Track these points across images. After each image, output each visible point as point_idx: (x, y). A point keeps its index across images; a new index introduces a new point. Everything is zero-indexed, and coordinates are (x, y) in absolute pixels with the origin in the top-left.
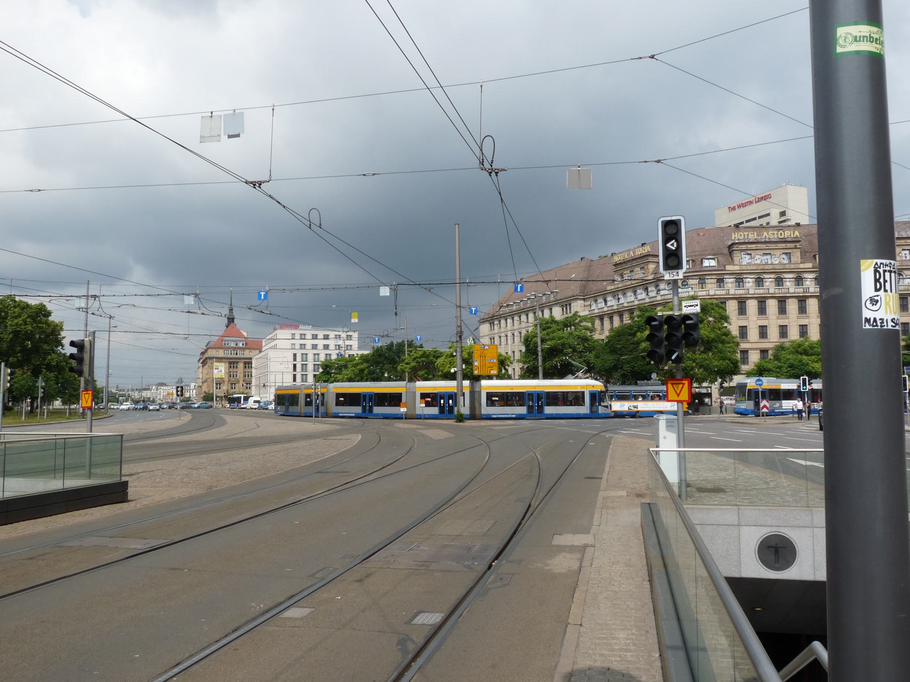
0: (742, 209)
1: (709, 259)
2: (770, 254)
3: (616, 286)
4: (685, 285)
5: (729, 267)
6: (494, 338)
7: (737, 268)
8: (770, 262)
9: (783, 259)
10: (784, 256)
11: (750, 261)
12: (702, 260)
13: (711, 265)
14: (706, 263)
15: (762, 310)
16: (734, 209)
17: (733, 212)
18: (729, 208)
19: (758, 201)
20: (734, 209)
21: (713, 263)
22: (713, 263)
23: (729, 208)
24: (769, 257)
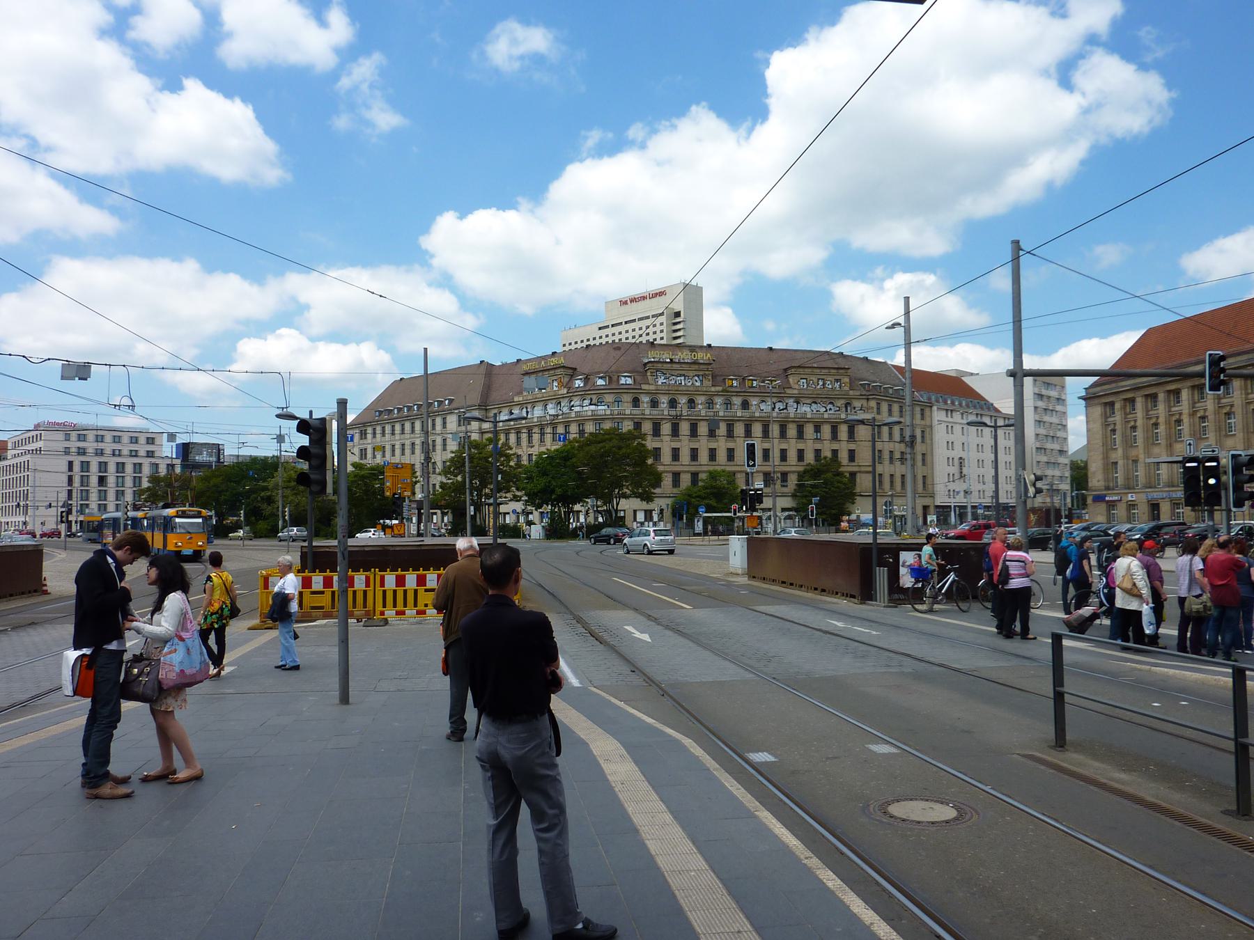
0: (634, 304)
1: (625, 376)
2: (684, 375)
3: (525, 398)
4: (601, 402)
5: (645, 387)
6: (366, 449)
7: (652, 387)
8: (683, 384)
9: (696, 381)
10: (696, 378)
11: (665, 381)
12: (618, 376)
13: (628, 383)
14: (623, 381)
15: (675, 432)
16: (626, 303)
17: (625, 307)
18: (621, 301)
19: (653, 297)
20: (626, 303)
21: (629, 381)
22: (629, 381)
23: (621, 301)
24: (683, 378)
